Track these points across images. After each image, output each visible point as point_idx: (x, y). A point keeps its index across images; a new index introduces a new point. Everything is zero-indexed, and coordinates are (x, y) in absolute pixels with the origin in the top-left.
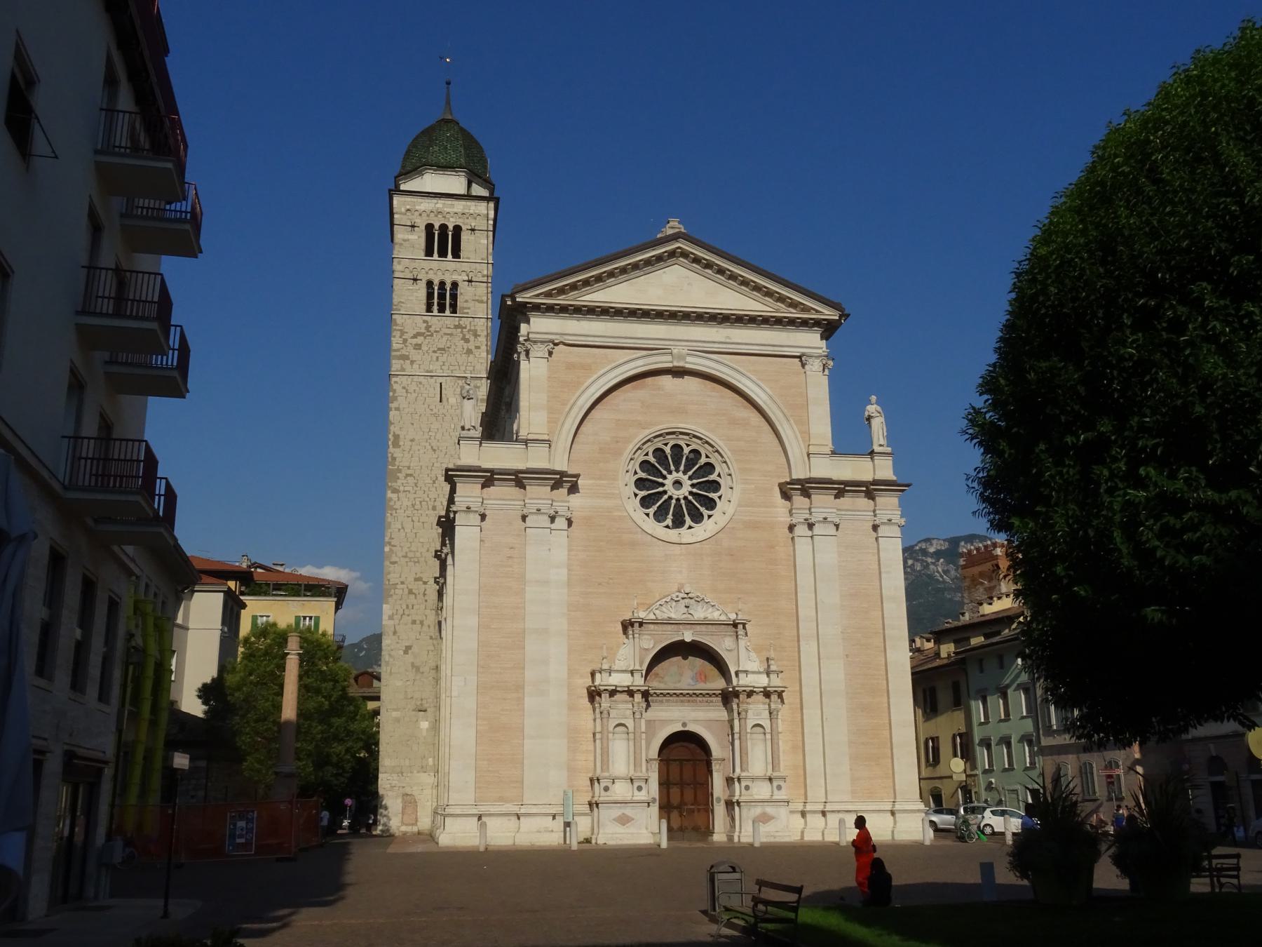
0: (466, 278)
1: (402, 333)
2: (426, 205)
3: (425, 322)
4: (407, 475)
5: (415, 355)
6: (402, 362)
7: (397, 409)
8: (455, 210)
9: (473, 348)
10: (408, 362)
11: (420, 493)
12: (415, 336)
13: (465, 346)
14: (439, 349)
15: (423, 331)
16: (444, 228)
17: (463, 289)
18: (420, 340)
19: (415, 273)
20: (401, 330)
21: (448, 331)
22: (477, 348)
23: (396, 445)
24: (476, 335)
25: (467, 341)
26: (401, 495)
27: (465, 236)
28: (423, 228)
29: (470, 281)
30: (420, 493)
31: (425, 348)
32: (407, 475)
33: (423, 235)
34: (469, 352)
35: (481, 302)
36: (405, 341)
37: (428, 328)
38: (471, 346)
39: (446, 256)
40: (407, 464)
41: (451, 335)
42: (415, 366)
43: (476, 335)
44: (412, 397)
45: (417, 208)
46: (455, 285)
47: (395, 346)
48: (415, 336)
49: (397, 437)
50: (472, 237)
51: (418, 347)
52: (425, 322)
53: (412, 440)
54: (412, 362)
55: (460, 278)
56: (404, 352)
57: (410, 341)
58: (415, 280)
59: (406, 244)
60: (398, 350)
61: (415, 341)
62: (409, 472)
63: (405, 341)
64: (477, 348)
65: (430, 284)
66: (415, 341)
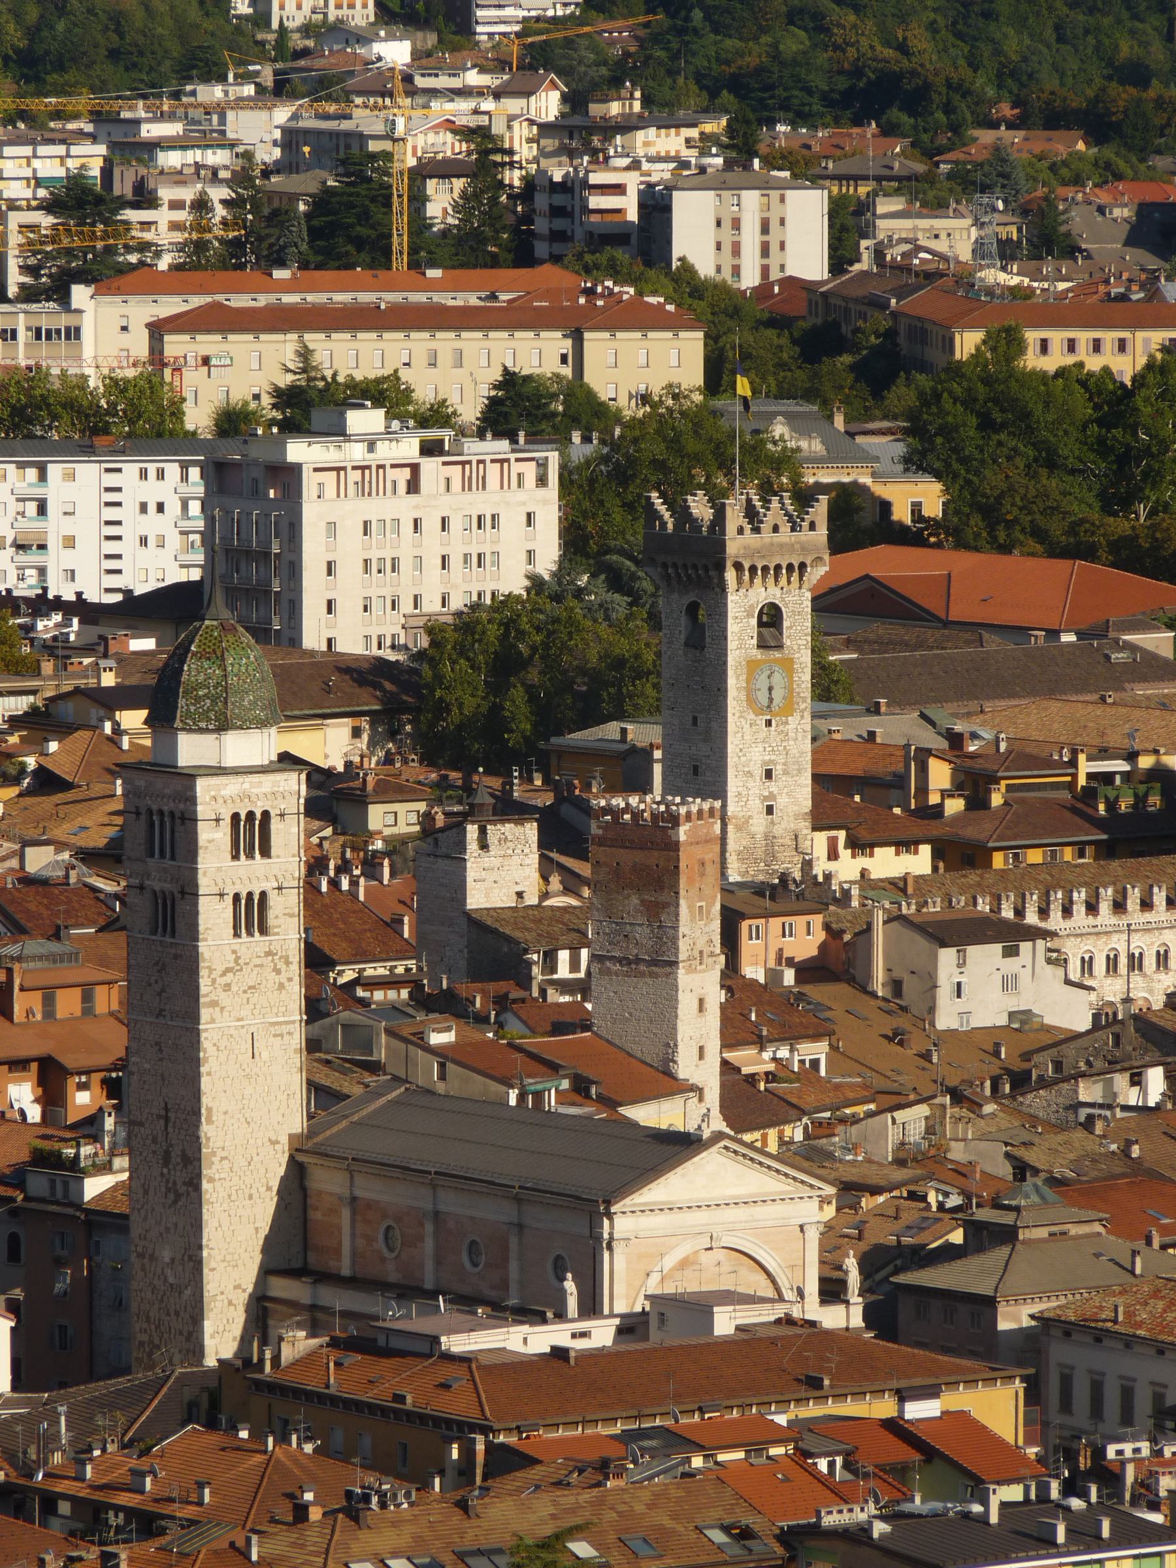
0: (275, 885)
1: (211, 970)
2: (231, 787)
3: (234, 952)
4: (223, 1159)
5: (224, 998)
6: (211, 1010)
7: (209, 1074)
8: (263, 790)
9: (284, 981)
10: (217, 1009)
11: (235, 1179)
12: (224, 974)
13: (277, 978)
14: (250, 988)
15: (232, 965)
16: (251, 815)
17: (274, 899)
18: (229, 977)
19: (221, 885)
20: (209, 968)
21: (258, 961)
22: (290, 980)
23: (210, 1121)
24: (288, 963)
25: (278, 972)
26: (217, 1184)
27: (275, 825)
28: (228, 820)
29: (280, 888)
30: (235, 1179)
31: (234, 988)
32: (223, 1159)
33: (228, 830)
34: (281, 987)
35: (291, 915)
36: (214, 981)
37: (237, 959)
38: (283, 978)
39: (253, 858)
40: (220, 1144)
41: (261, 966)
42: (226, 1014)
43: (288, 963)
44: (223, 1057)
45: (223, 793)
46: (263, 894)
47: (203, 990)
48: (224, 974)
49: (209, 1110)
50: (281, 826)
51: (227, 987)
52: (234, 952)
53: (226, 1113)
54: (222, 1009)
55: (269, 886)
56: (213, 997)
57: (219, 980)
58: (221, 895)
59: (211, 846)
60: (206, 995)
61: (223, 981)
62: (224, 1154)
63: (214, 981)
64: (290, 980)
65: (237, 898)
66: (223, 981)
